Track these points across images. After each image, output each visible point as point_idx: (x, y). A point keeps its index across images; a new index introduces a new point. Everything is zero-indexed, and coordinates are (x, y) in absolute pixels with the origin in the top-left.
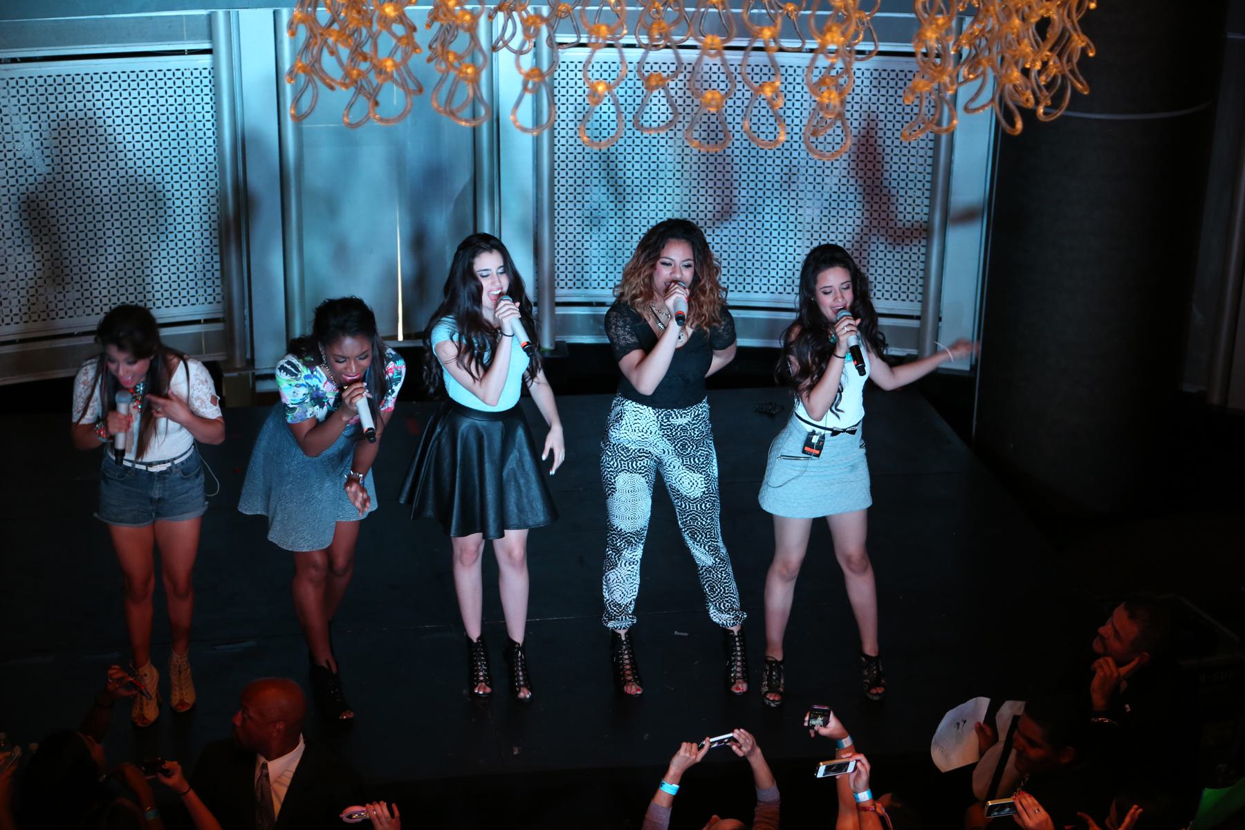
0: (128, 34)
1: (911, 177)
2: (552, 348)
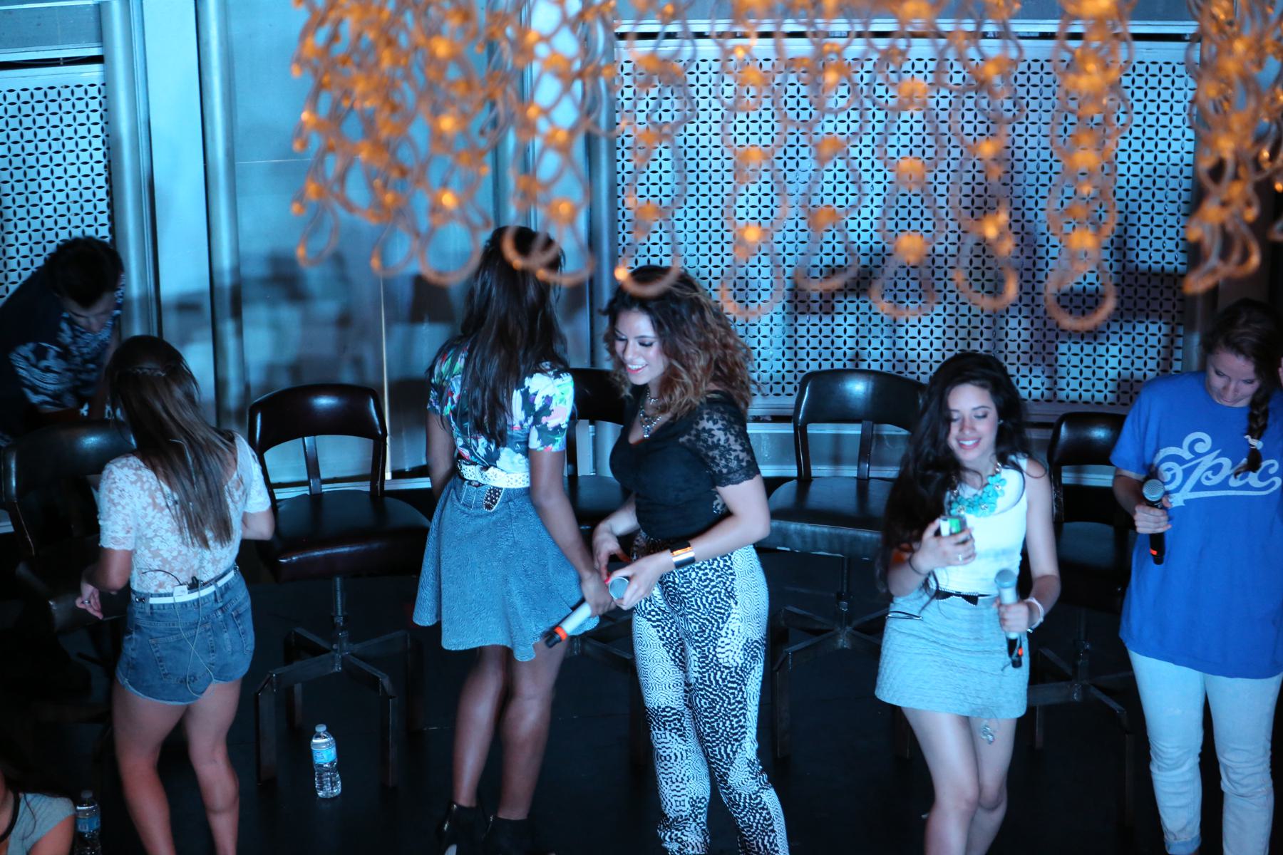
1: (1158, 220)
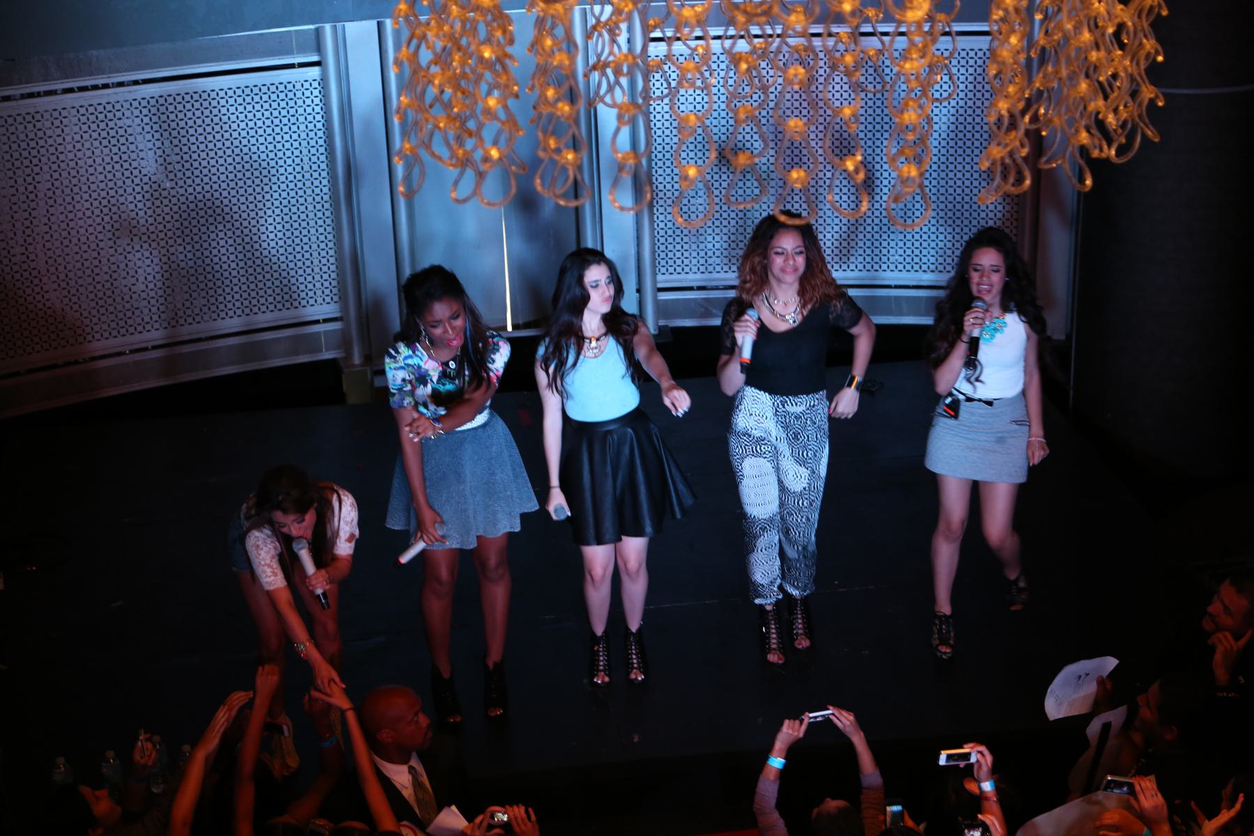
0: (242, 51)
2: (656, 333)
